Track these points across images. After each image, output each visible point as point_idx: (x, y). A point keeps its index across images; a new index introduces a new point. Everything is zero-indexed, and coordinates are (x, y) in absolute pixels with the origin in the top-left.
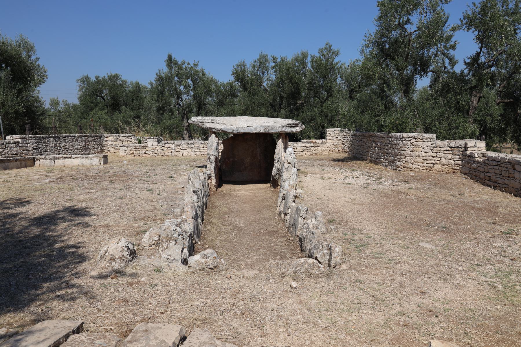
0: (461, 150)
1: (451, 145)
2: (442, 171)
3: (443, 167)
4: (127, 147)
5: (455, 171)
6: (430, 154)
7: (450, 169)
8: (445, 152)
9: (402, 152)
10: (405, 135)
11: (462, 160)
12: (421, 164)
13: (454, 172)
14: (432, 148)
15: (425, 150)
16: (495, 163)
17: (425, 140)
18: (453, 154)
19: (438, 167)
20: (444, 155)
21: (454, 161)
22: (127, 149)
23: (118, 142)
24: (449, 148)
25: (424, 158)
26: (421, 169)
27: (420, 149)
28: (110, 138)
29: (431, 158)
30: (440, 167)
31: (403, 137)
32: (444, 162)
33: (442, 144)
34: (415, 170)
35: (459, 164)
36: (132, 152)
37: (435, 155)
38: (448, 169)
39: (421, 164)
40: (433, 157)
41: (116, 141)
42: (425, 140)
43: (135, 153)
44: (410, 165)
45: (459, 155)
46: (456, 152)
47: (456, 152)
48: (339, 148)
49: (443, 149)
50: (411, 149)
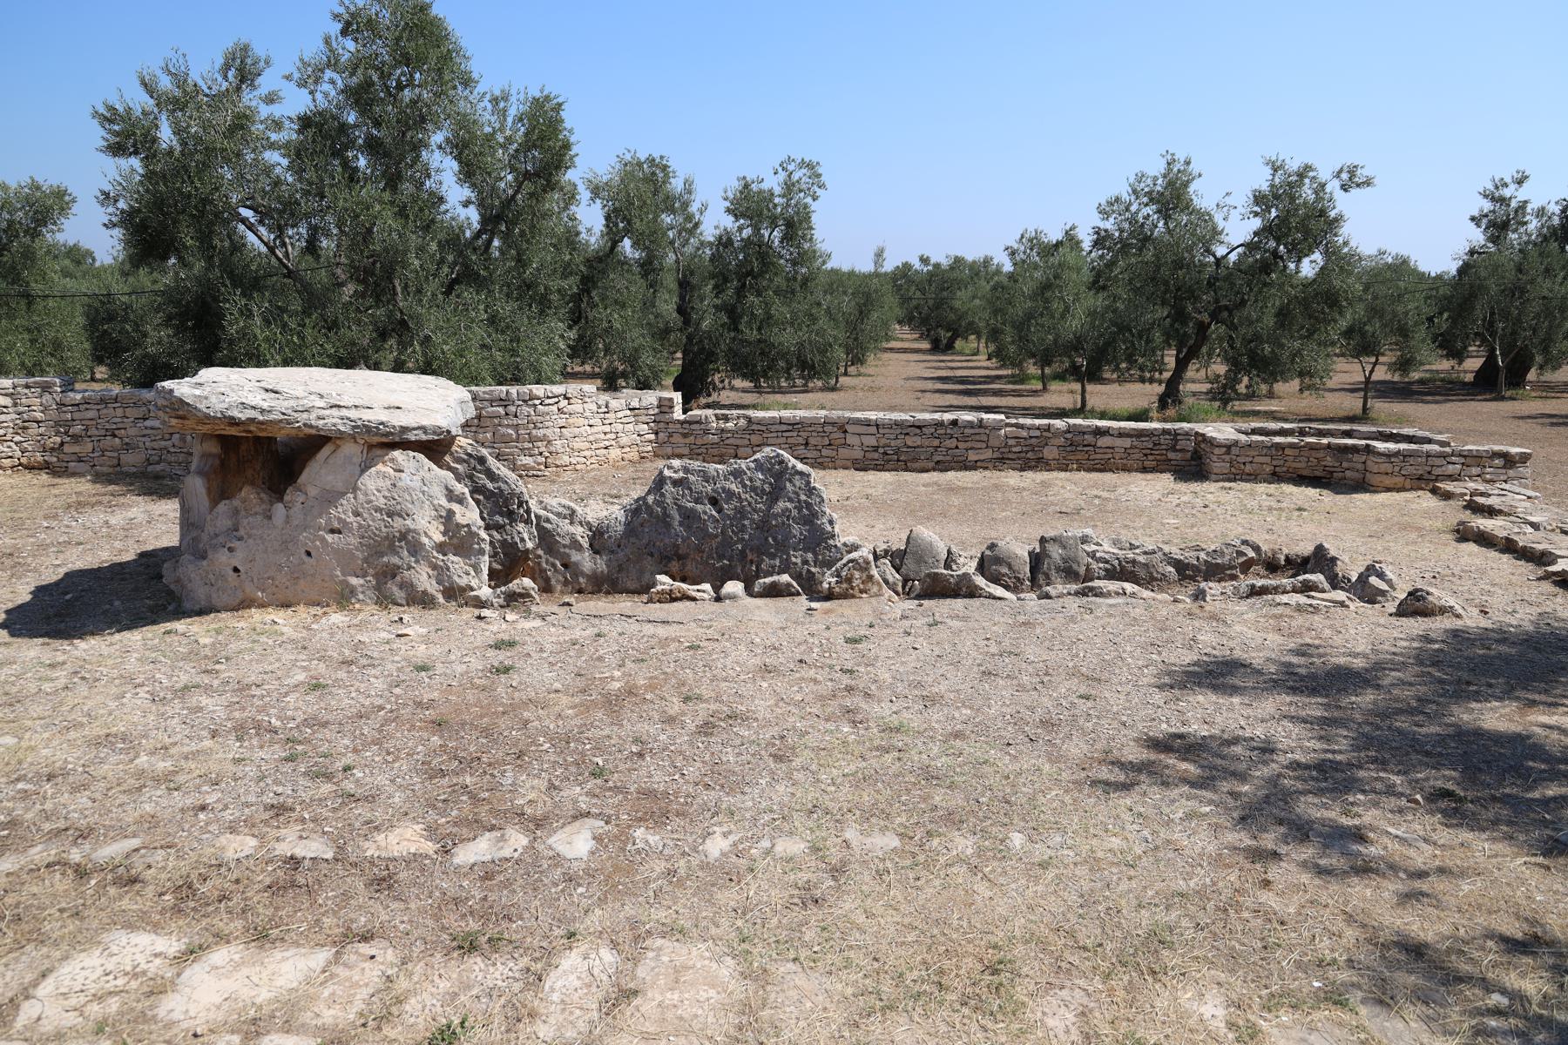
1: (635, 404)
7: (634, 455)
10: (538, 390)
11: (656, 434)
16: (784, 428)
19: (615, 453)
25: (591, 438)
27: (581, 421)
30: (618, 451)
32: (624, 440)
37: (607, 428)
44: (566, 459)
49: (620, 415)
50: (562, 422)
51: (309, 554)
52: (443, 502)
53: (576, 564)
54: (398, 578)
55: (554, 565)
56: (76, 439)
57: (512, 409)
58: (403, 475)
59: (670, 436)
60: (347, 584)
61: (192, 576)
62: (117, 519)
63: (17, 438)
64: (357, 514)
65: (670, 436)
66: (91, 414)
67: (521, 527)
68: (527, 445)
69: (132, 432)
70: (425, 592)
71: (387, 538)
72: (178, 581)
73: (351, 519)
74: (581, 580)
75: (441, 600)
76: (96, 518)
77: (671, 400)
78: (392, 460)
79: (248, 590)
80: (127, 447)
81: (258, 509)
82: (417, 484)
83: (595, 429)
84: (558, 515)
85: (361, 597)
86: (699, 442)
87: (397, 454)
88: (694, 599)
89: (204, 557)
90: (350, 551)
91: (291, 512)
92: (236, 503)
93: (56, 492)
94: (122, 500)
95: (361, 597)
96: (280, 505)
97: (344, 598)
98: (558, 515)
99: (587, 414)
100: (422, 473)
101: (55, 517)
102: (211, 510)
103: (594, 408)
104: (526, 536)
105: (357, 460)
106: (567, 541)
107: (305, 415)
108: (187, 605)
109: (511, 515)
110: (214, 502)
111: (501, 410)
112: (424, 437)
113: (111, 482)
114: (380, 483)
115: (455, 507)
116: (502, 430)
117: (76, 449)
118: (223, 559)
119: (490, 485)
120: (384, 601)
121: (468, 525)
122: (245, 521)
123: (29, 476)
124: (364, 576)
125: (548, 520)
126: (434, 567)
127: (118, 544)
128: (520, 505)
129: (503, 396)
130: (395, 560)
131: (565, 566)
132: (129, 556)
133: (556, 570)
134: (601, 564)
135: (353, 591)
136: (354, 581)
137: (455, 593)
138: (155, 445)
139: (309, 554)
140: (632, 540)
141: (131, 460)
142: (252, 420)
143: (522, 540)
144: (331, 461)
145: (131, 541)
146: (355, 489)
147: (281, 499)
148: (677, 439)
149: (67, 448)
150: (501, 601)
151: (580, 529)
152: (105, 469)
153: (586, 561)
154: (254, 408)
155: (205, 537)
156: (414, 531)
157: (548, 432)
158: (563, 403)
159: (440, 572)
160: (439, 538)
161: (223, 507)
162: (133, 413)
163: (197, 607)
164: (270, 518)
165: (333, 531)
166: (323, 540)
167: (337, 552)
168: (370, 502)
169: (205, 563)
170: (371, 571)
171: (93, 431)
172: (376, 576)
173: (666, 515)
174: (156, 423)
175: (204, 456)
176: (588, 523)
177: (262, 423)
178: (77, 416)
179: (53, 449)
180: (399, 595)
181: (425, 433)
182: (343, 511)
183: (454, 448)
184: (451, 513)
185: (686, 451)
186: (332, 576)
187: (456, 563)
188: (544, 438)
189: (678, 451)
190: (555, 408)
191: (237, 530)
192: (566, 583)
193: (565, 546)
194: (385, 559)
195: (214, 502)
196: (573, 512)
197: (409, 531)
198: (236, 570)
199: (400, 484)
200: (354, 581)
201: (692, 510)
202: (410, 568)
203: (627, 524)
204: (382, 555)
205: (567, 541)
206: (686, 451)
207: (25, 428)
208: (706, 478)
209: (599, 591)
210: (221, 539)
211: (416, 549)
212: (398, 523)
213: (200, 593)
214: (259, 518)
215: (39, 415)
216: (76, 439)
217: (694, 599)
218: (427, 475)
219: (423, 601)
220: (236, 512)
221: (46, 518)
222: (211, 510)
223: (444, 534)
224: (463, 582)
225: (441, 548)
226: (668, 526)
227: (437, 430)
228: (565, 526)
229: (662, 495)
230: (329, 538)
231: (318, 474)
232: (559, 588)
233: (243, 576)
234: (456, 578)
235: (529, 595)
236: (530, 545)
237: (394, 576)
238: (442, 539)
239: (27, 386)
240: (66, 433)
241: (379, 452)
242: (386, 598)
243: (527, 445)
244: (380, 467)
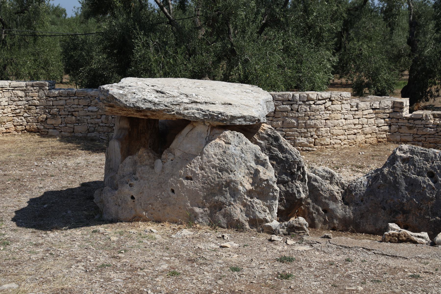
0: (388, 112)
1: (376, 105)
2: (366, 142)
3: (367, 136)
5: (381, 140)
6: (351, 121)
7: (373, 140)
8: (368, 116)
9: (312, 122)
10: (313, 95)
11: (390, 126)
12: (342, 137)
13: (380, 142)
14: (354, 112)
15: (346, 117)
17: (344, 102)
18: (377, 118)
19: (361, 138)
20: (366, 120)
21: (377, 126)
24: (371, 111)
25: (345, 127)
26: (342, 144)
29: (353, 126)
30: (363, 137)
31: (309, 99)
32: (367, 129)
33: (365, 106)
34: (336, 146)
35: (385, 131)
37: (356, 121)
38: (372, 139)
39: (342, 137)
40: (355, 125)
42: (344, 102)
44: (328, 140)
45: (384, 119)
46: (382, 115)
47: (382, 115)
48: (9, 125)
49: (366, 112)
50: (327, 116)
51: (173, 191)
52: (253, 164)
53: (333, 211)
54: (223, 210)
55: (318, 210)
56: (54, 116)
57: (296, 106)
58: (230, 146)
59: (400, 128)
60: (192, 211)
61: (109, 198)
62: (71, 163)
63: (26, 115)
64: (202, 169)
65: (400, 128)
66: (62, 102)
67: (298, 183)
68: (303, 130)
69: (81, 113)
70: (238, 221)
71: (218, 185)
72: (102, 202)
73: (198, 171)
74: (335, 221)
75: (248, 227)
76: (60, 161)
77: (402, 103)
78: (225, 136)
79: (138, 210)
80: (79, 122)
81: (147, 162)
82: (238, 152)
83: (348, 122)
84: (322, 177)
85: (201, 220)
86: (420, 133)
87: (227, 133)
88: (415, 242)
89: (116, 189)
90: (196, 191)
91: (165, 165)
92: (136, 157)
93: (41, 145)
94: (74, 152)
95: (201, 220)
96: (159, 161)
97: (190, 220)
98: (322, 177)
99: (344, 111)
100: (241, 145)
101: (41, 160)
102: (122, 162)
103: (348, 107)
104: (301, 189)
105: (204, 136)
106: (327, 195)
107: (177, 107)
108: (105, 216)
109: (292, 175)
110: (124, 157)
111: (288, 107)
112: (244, 123)
113: (69, 142)
114: (217, 150)
115: (260, 168)
116: (288, 120)
117: (53, 122)
118: (126, 191)
119: (281, 155)
120: (214, 224)
121: (267, 180)
122: (140, 169)
123: (30, 136)
124: (203, 208)
125: (316, 180)
126: (245, 205)
127: (71, 178)
128: (299, 169)
129: (290, 98)
130: (222, 199)
131: (325, 211)
132: (76, 185)
133: (319, 213)
134: (349, 212)
135: (196, 216)
136: (197, 210)
137: (257, 224)
138: (93, 121)
139: (173, 191)
140: (371, 197)
141: (80, 129)
142: (149, 109)
143: (299, 192)
144: (189, 135)
145: (77, 177)
146: (202, 153)
147: (160, 157)
148: (404, 130)
149: (49, 122)
150: (285, 231)
151: (336, 188)
152: (66, 134)
153: (339, 209)
154: (150, 102)
155: (118, 177)
156: (235, 181)
157: (317, 122)
158: (329, 104)
159: (248, 209)
160: (248, 187)
161: (128, 160)
162: (83, 102)
163: (110, 218)
164: (153, 168)
165: (187, 178)
166: (182, 183)
167: (189, 191)
168: (210, 161)
169: (116, 192)
170: (207, 204)
171: (62, 112)
172: (210, 208)
173: (396, 181)
174: (95, 109)
175: (121, 129)
176: (342, 184)
177: (154, 111)
178: (55, 103)
179: (42, 121)
180: (223, 221)
181: (245, 120)
182: (194, 166)
183: (260, 130)
184: (257, 172)
185: (410, 139)
186: (185, 206)
187: (258, 203)
188: (315, 126)
189: (404, 138)
190: (323, 107)
191: (135, 174)
192: (325, 222)
193: (326, 198)
194: (216, 198)
195: (124, 157)
196: (333, 176)
197: (231, 181)
198: (133, 198)
199: (228, 151)
200: (197, 210)
201: (415, 180)
202: (230, 204)
203: (369, 187)
204: (214, 195)
205: (327, 195)
206: (410, 139)
207: (30, 109)
208: (427, 158)
209: (347, 230)
210: (126, 179)
211: (235, 193)
212: (225, 176)
213: (113, 209)
214: (147, 167)
215: (37, 102)
216: (54, 116)
217: (415, 242)
218: (245, 147)
219: (237, 226)
220: (135, 163)
221: (36, 160)
222: (122, 162)
223: (252, 184)
224: (261, 216)
225: (250, 193)
226: (397, 189)
227: (252, 119)
228: (327, 185)
229: (394, 168)
230: (185, 182)
231: (182, 143)
232: (320, 225)
233: (136, 202)
234: (257, 213)
235: (302, 229)
236: (303, 195)
237: (220, 209)
238: (251, 188)
239: (33, 86)
240: (49, 113)
241: (217, 131)
242: (215, 222)
243: (303, 130)
244: (217, 140)
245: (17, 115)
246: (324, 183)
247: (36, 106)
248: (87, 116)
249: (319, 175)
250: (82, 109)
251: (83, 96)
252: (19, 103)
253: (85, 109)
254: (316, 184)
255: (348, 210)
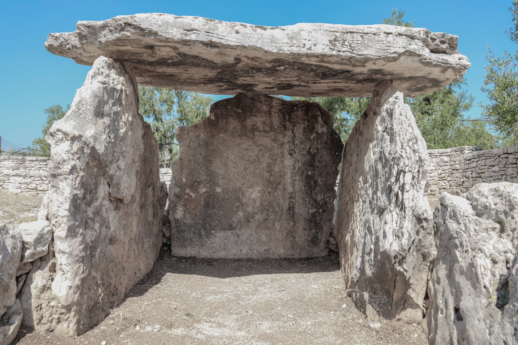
4: (25, 177)
22: (24, 181)
23: (22, 170)
28: (6, 163)
36: (33, 186)
41: (18, 169)
43: (39, 188)
63: (449, 179)
66: (474, 164)
104: (389, 228)
125: (454, 216)
162: (489, 162)
215: (458, 166)
245: (442, 179)
246: (472, 227)
247: (457, 170)
248: (491, 177)
249: (474, 208)
250: (487, 170)
251: (489, 155)
252: (445, 168)
253: (490, 170)
254: (453, 225)
255: (497, 328)
